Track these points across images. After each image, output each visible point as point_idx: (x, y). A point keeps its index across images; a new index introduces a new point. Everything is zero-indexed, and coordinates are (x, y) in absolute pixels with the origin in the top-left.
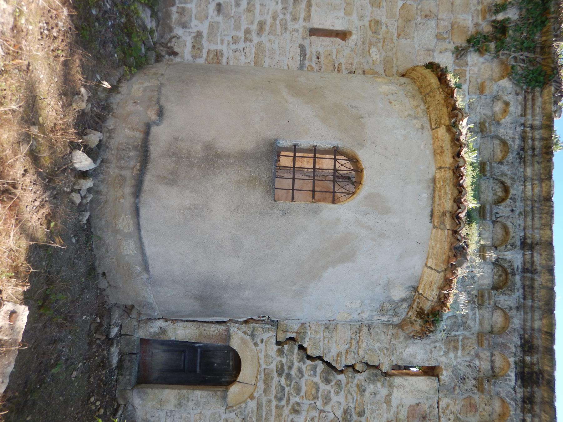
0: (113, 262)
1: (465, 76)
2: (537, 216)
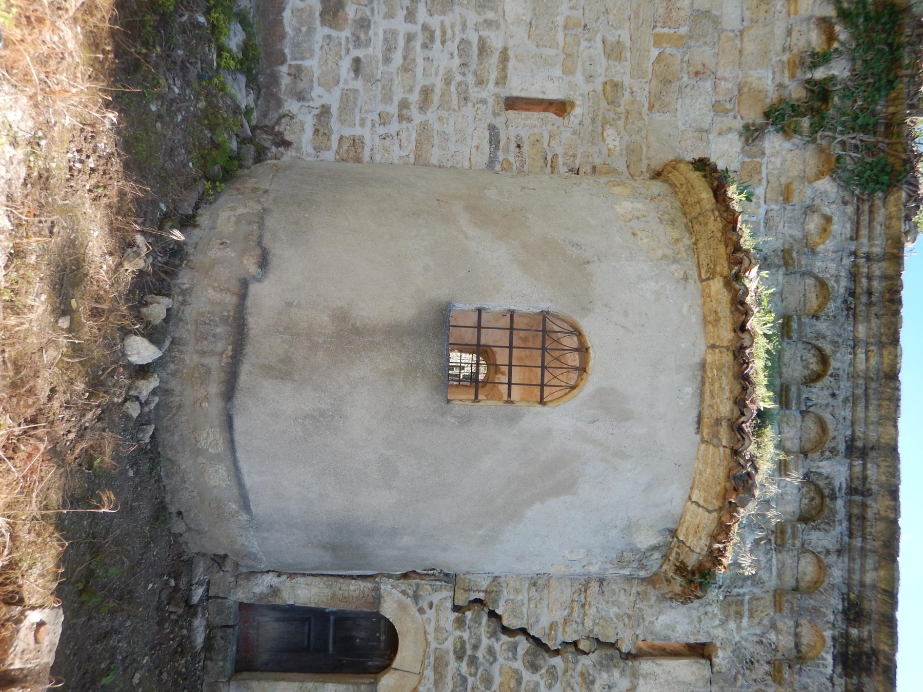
0: (193, 497)
1: (760, 173)
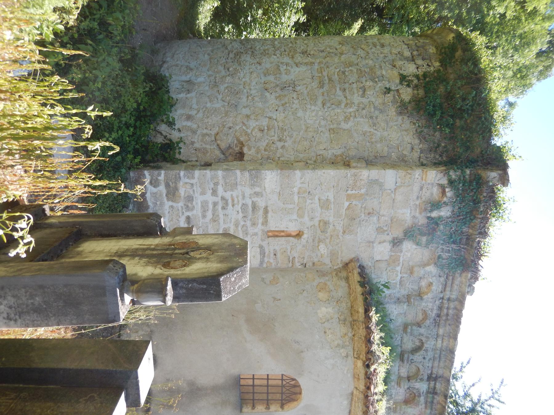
1: (399, 260)
2: (443, 359)
